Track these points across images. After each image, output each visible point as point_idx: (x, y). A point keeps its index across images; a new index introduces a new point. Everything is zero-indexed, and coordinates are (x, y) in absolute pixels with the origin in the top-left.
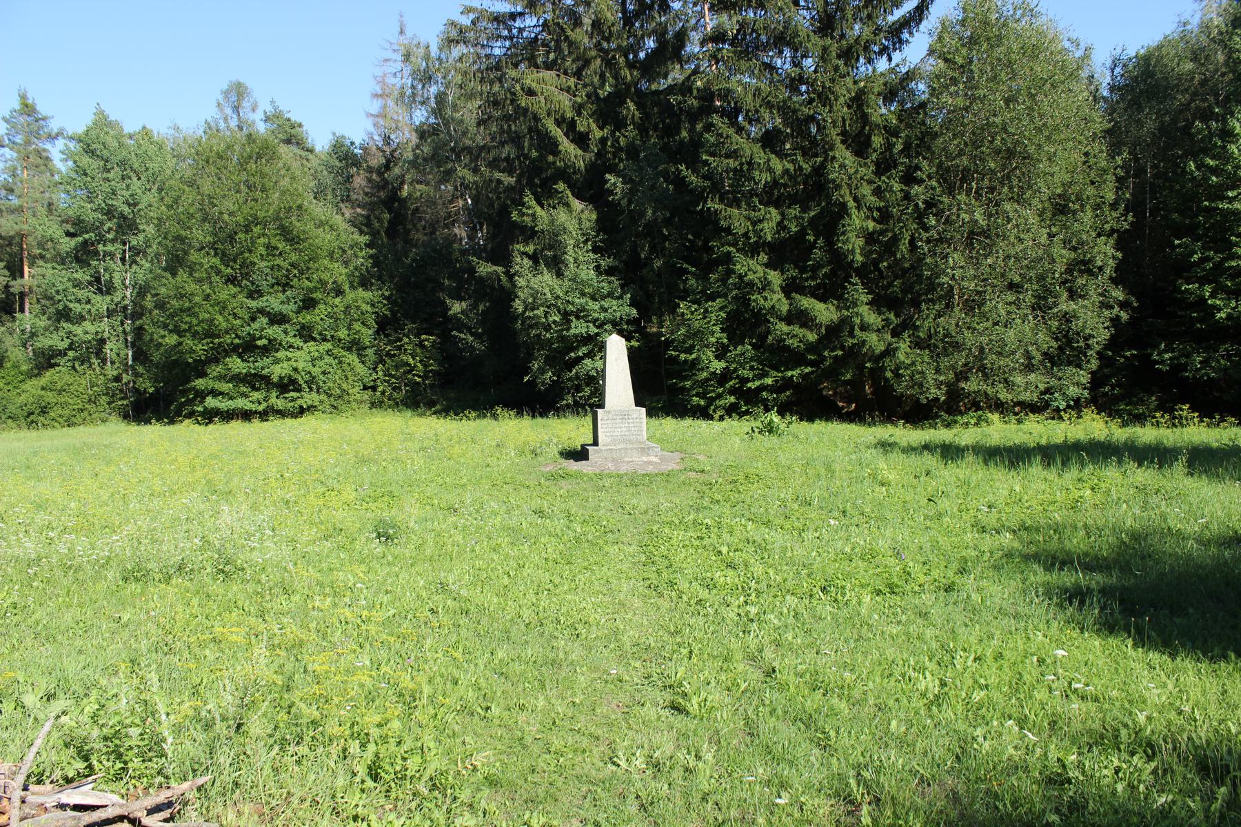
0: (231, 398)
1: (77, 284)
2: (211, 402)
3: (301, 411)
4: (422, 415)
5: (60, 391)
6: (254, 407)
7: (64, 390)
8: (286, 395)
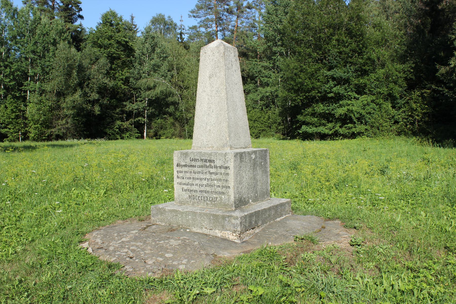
0: (316, 127)
1: (266, 68)
2: (304, 128)
3: (353, 136)
4: (327, 142)
5: (255, 121)
6: (327, 131)
7: (257, 120)
8: (346, 126)
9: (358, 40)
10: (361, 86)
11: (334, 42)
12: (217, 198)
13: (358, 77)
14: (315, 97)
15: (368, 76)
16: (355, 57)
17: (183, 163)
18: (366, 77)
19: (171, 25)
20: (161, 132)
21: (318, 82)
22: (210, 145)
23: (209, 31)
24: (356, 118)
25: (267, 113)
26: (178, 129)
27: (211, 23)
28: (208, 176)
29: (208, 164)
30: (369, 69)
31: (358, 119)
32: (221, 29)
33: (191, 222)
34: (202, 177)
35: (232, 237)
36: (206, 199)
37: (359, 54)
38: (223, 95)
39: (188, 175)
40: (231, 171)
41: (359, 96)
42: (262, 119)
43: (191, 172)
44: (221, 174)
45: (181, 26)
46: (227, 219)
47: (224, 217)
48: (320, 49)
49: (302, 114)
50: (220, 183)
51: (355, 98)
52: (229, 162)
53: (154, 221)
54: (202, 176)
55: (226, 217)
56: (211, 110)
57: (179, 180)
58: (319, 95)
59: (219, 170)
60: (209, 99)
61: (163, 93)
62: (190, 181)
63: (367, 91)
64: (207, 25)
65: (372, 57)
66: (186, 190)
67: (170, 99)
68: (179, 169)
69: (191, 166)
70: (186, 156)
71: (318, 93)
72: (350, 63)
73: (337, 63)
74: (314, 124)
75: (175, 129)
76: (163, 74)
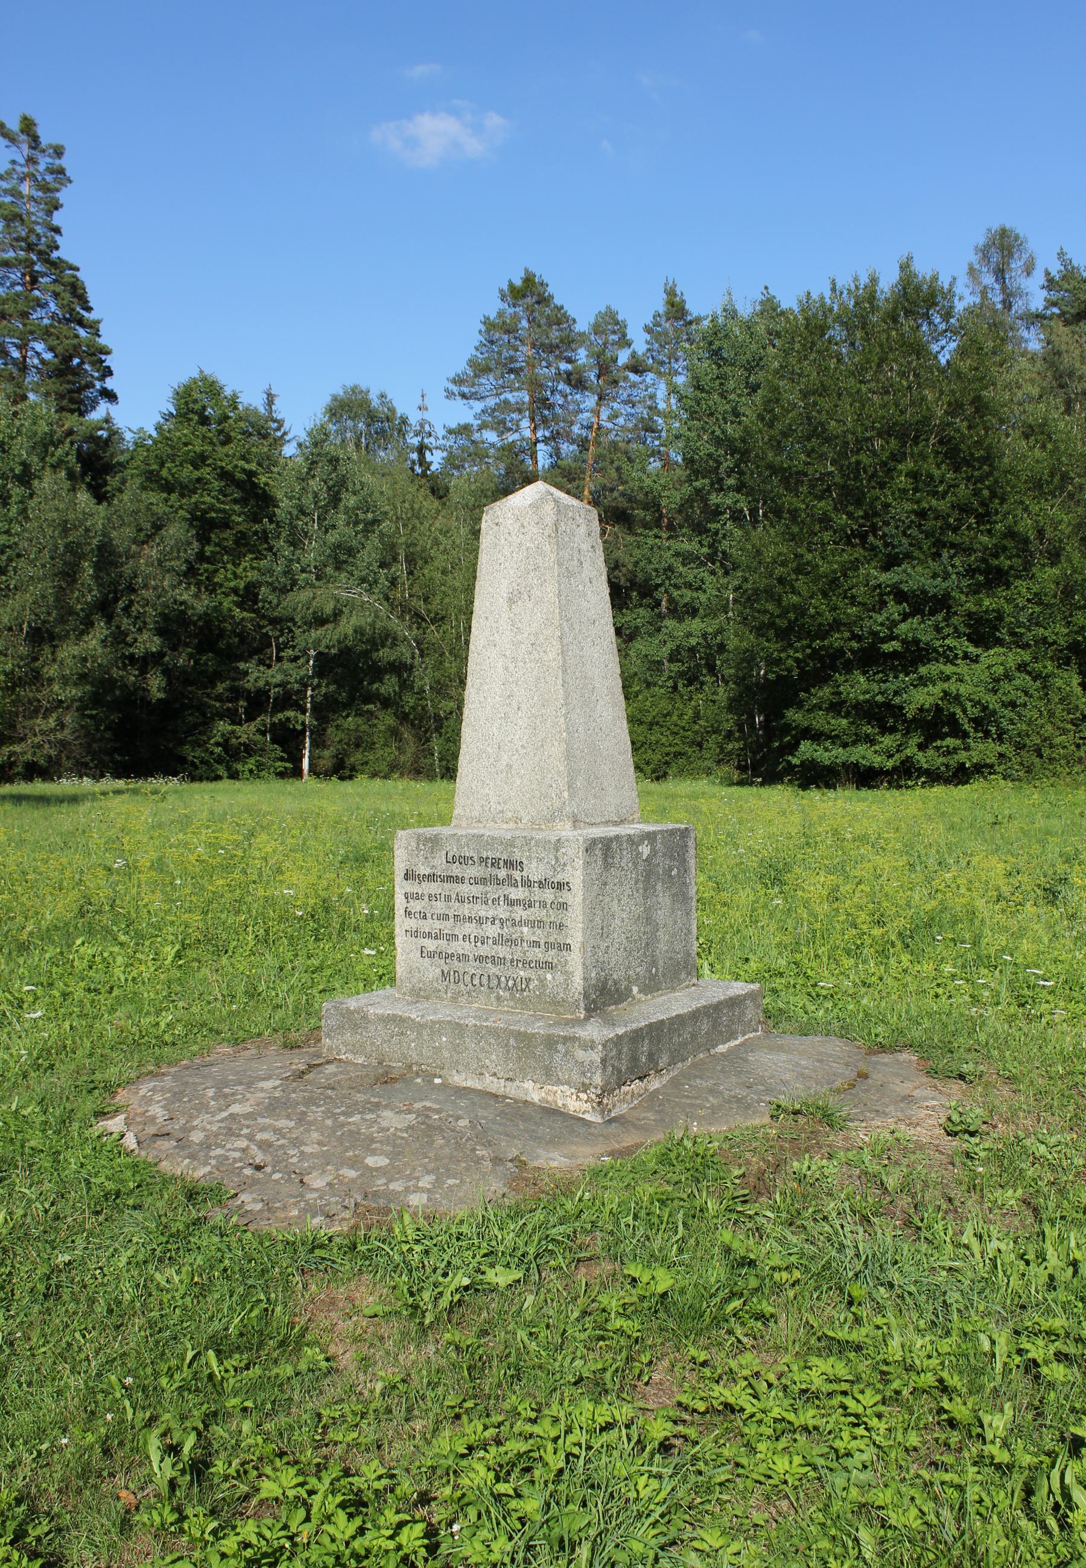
0: (845, 745)
1: (687, 558)
2: (806, 749)
3: (961, 775)
4: (878, 793)
5: (651, 724)
6: (877, 761)
7: (657, 723)
8: (939, 743)
9: (976, 473)
10: (987, 620)
11: (902, 481)
12: (528, 980)
13: (975, 590)
14: (841, 652)
15: (1008, 588)
16: (969, 528)
17: (424, 870)
18: (1001, 592)
19: (388, 419)
20: (356, 758)
21: (852, 604)
22: (510, 815)
23: (510, 439)
24: (971, 720)
25: (690, 699)
26: (411, 749)
27: (515, 416)
28: (502, 912)
29: (502, 873)
30: (1011, 567)
31: (977, 722)
32: (547, 434)
33: (446, 1054)
34: (482, 914)
35: (576, 1104)
36: (495, 982)
37: (981, 518)
38: (551, 656)
39: (440, 907)
40: (576, 898)
41: (979, 651)
42: (675, 718)
43: (448, 898)
44: (543, 904)
45: (422, 426)
46: (560, 1047)
47: (551, 1043)
48: (858, 503)
49: (800, 705)
50: (539, 935)
51: (966, 656)
52: (568, 867)
53: (330, 1049)
54: (483, 911)
55: (557, 1042)
56: (515, 706)
57: (412, 923)
58: (855, 645)
59: (537, 894)
60: (506, 669)
61: (362, 635)
62: (447, 926)
63: (1003, 634)
64: (503, 422)
65: (1020, 528)
66: (431, 955)
67: (385, 654)
68: (412, 887)
69: (451, 879)
70: (432, 848)
71: (850, 639)
72: (953, 545)
73: (911, 545)
74: (837, 736)
75: (399, 749)
76: (364, 573)
